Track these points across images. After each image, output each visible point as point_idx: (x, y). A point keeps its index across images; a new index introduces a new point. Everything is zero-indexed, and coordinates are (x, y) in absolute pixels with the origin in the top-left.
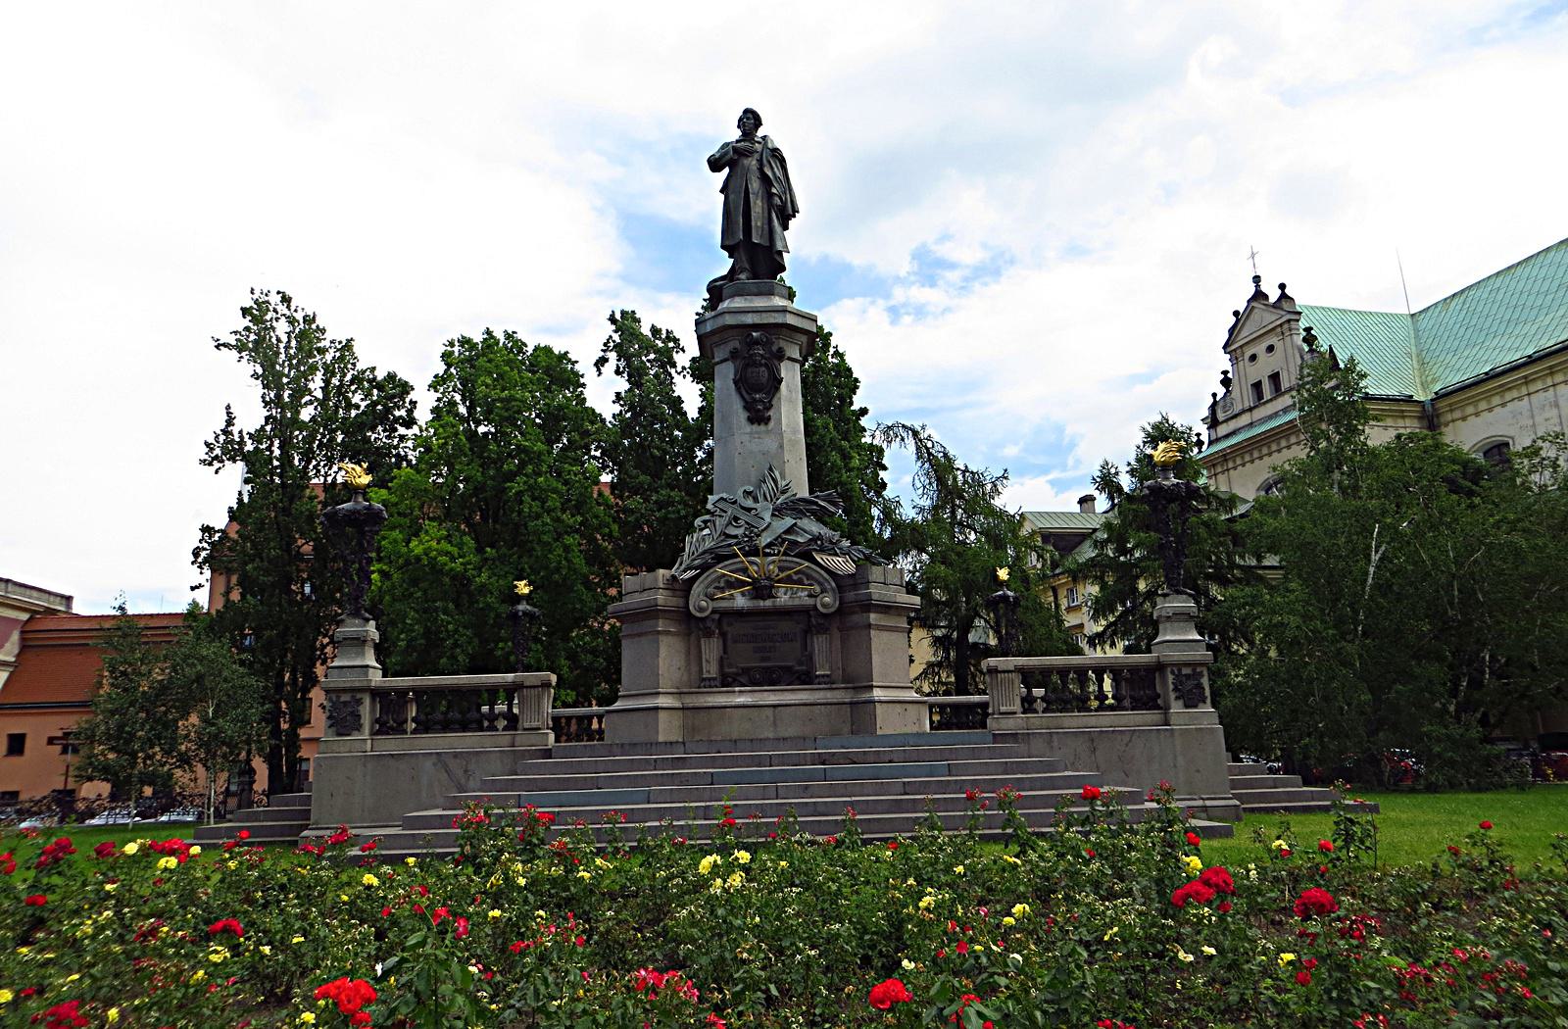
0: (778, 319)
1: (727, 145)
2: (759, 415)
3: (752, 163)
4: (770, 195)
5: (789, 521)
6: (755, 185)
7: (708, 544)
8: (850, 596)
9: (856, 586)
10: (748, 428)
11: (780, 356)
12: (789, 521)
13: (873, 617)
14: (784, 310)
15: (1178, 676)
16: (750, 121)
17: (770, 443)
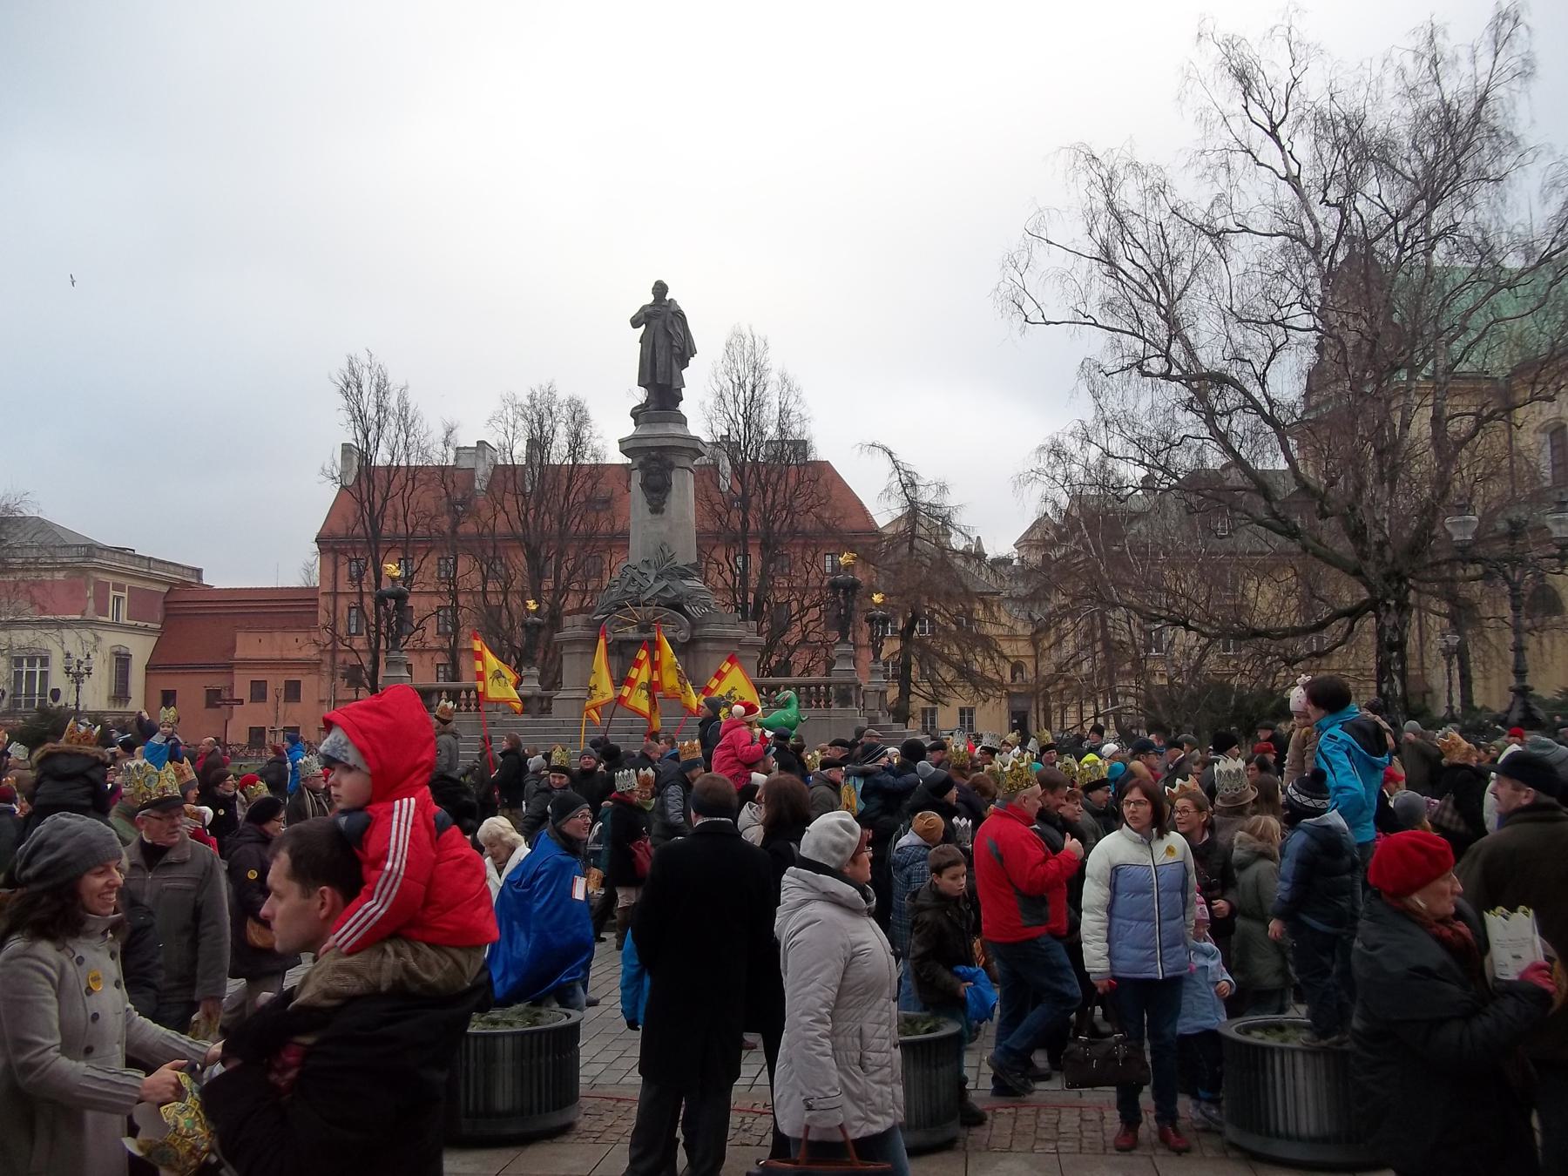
0: (669, 442)
1: (644, 308)
2: (657, 508)
3: (656, 323)
4: (672, 346)
5: (664, 583)
6: (661, 341)
7: (614, 598)
8: (697, 633)
9: (702, 625)
10: (649, 516)
11: (671, 467)
12: (664, 583)
13: (710, 646)
14: (673, 437)
15: (838, 691)
16: (660, 289)
17: (664, 528)
